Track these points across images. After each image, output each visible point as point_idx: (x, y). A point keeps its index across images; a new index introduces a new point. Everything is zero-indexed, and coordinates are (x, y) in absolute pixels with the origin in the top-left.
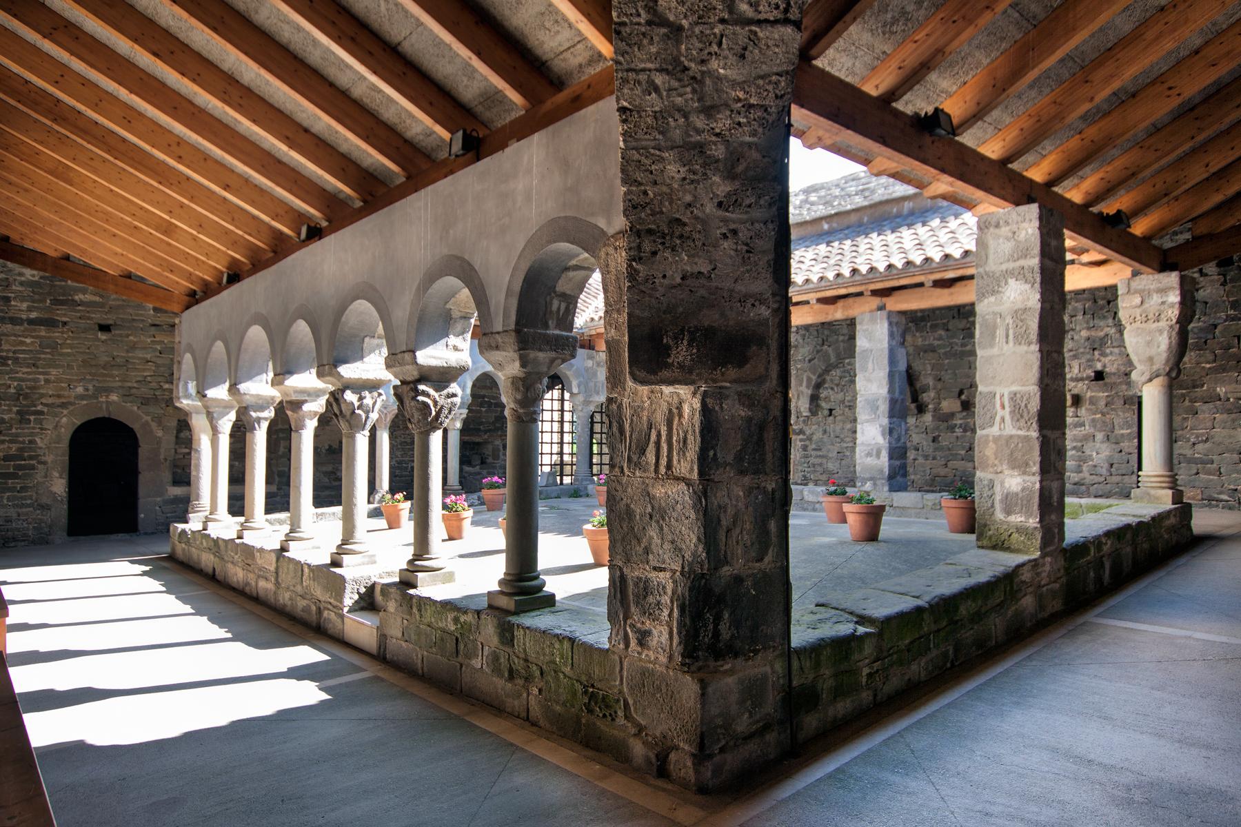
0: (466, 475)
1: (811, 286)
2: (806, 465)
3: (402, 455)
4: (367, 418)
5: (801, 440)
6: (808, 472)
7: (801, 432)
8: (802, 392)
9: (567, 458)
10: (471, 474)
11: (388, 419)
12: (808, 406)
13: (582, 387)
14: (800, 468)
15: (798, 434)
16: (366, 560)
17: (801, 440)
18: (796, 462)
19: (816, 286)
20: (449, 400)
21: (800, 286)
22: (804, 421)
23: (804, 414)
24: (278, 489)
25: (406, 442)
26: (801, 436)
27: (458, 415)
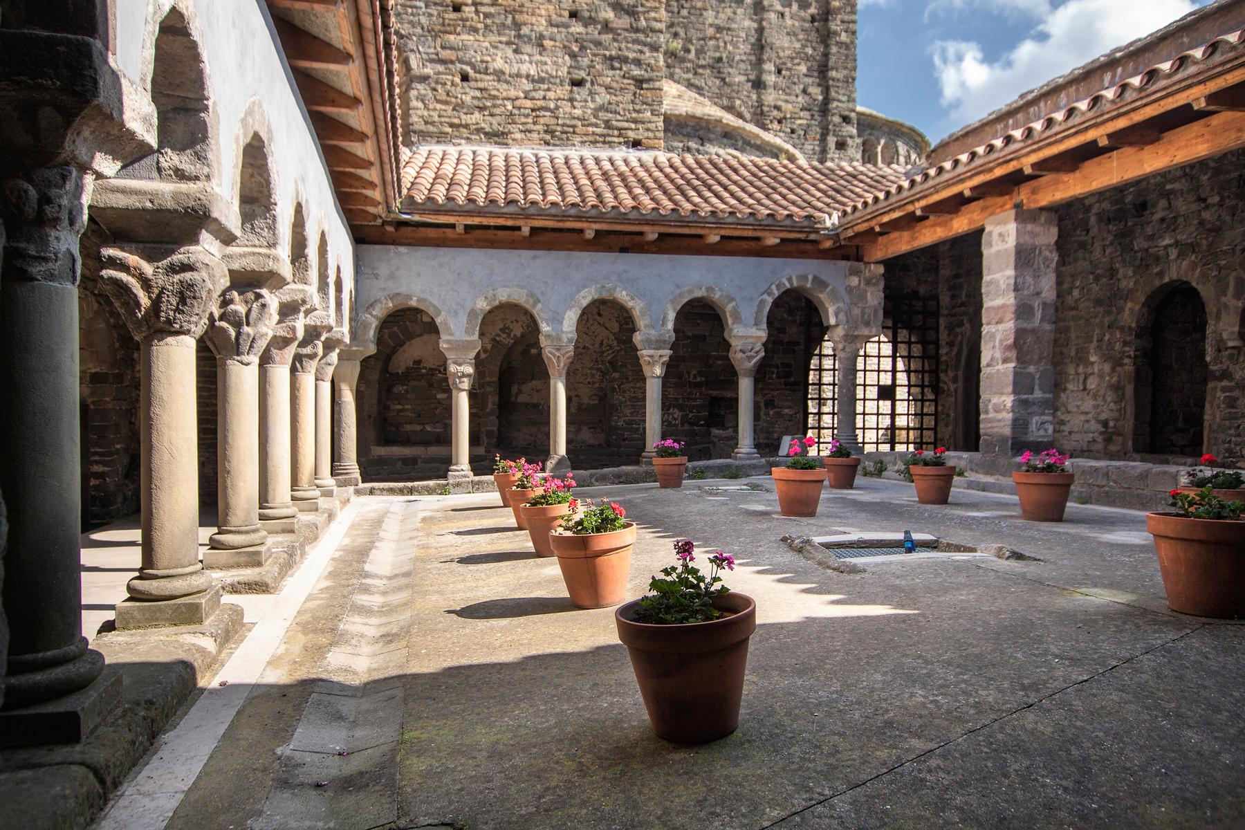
0: (715, 440)
1: (1192, 70)
2: (1232, 431)
3: (631, 413)
4: (239, 334)
5: (1224, 390)
6: (1236, 444)
7: (1226, 375)
8: (1226, 306)
9: (901, 422)
10: (720, 439)
11: (562, 365)
12: (1236, 329)
13: (842, 316)
14: (1223, 436)
15: (1220, 379)
16: (243, 559)
17: (1224, 390)
18: (1215, 427)
19: (1202, 67)
20: (177, 278)
21: (1170, 76)
22: (1231, 357)
23: (1231, 344)
24: (486, 452)
25: (634, 397)
26: (1225, 383)
27: (656, 358)
